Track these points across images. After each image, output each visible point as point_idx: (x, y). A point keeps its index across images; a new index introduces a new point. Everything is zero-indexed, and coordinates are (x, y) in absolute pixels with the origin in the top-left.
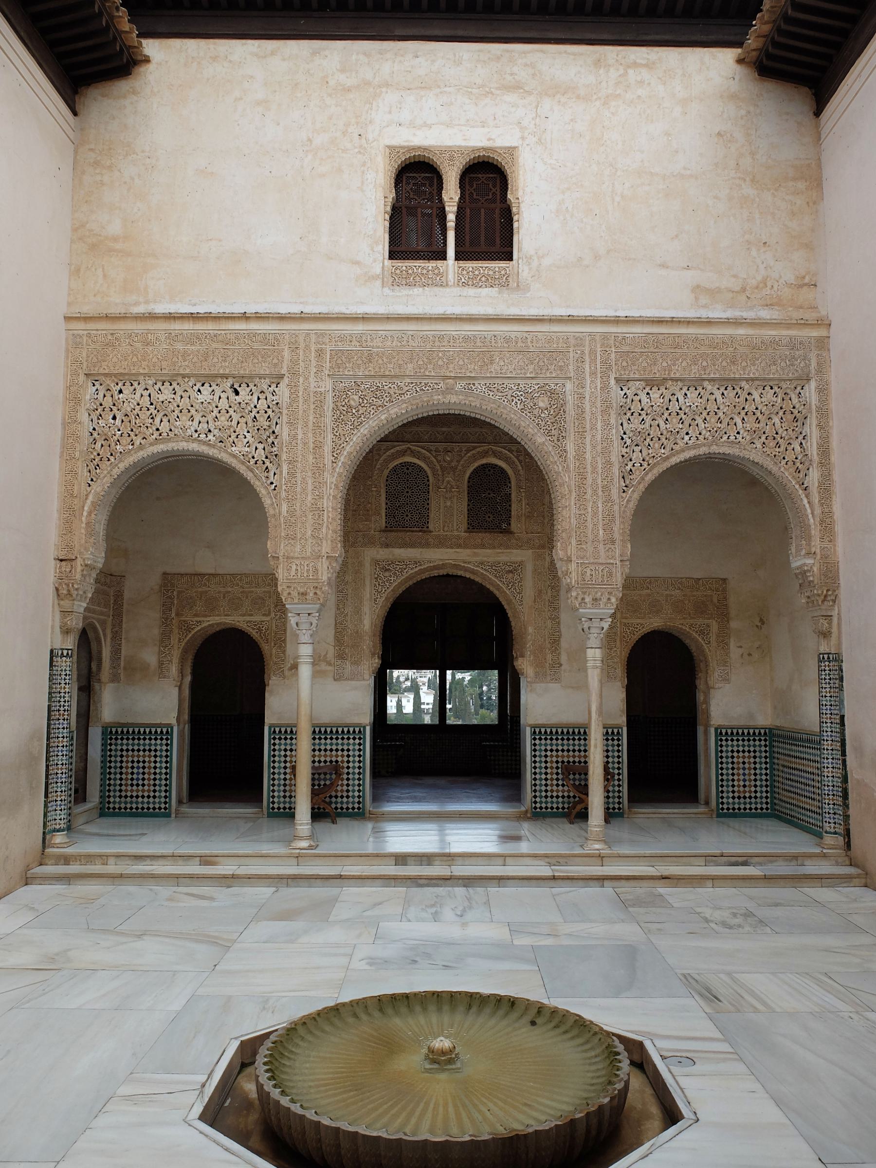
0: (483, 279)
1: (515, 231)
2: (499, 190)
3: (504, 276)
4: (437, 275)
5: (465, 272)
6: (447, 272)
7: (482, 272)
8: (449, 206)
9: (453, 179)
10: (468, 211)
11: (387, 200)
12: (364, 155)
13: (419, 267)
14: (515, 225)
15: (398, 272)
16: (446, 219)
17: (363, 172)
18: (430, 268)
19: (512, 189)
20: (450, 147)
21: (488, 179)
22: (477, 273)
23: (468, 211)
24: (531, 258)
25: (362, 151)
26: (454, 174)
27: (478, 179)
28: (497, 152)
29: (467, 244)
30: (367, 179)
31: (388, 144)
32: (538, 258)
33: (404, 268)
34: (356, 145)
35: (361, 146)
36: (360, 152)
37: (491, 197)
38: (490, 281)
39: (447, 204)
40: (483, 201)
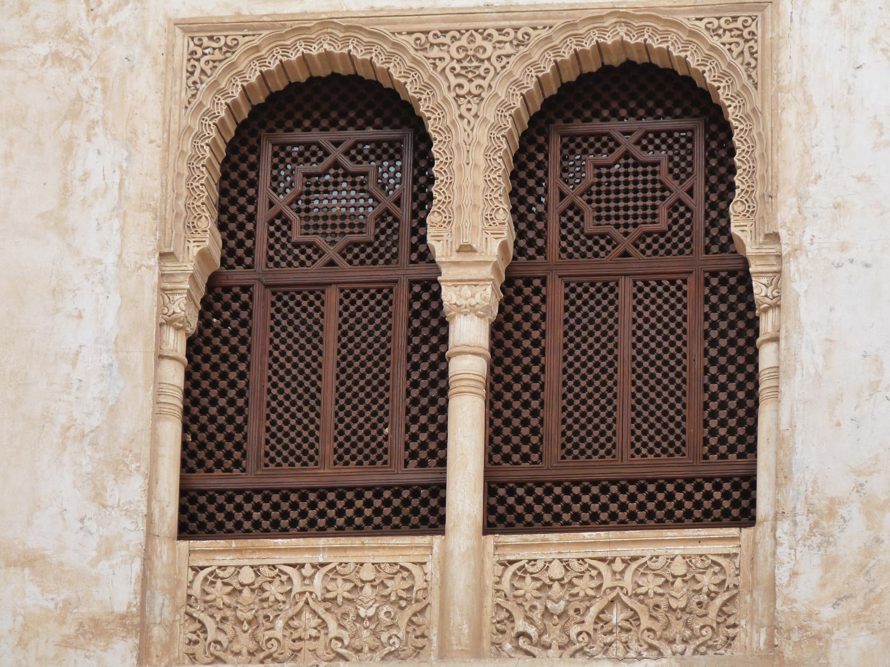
0: (616, 616)
1: (765, 384)
2: (700, 189)
3: (711, 595)
4: (400, 603)
5: (529, 586)
6: (443, 584)
7: (608, 582)
8: (458, 282)
9: (479, 157)
10: (556, 292)
11: (170, 267)
12: (76, 67)
13: (317, 567)
14: (767, 357)
15: (218, 592)
16: (445, 339)
17: (69, 147)
18: (367, 573)
19: (749, 192)
20: (464, 14)
21: (646, 140)
22: (585, 586)
23: (556, 292)
24: (831, 514)
25: (67, 51)
26: (482, 134)
27: (607, 142)
28: (679, 25)
29: (553, 448)
30: (86, 177)
31: (185, 13)
32: (868, 515)
33: (247, 576)
34: (41, 24)
35: (63, 30)
36: (57, 58)
37: (662, 223)
38: (645, 622)
39: (447, 274)
40: (626, 244)
